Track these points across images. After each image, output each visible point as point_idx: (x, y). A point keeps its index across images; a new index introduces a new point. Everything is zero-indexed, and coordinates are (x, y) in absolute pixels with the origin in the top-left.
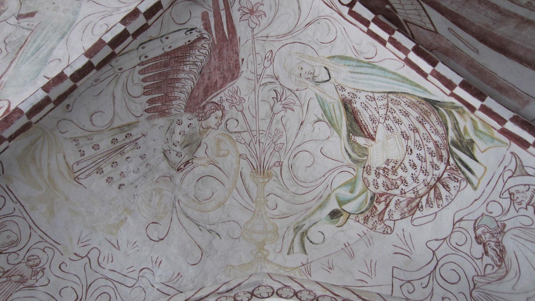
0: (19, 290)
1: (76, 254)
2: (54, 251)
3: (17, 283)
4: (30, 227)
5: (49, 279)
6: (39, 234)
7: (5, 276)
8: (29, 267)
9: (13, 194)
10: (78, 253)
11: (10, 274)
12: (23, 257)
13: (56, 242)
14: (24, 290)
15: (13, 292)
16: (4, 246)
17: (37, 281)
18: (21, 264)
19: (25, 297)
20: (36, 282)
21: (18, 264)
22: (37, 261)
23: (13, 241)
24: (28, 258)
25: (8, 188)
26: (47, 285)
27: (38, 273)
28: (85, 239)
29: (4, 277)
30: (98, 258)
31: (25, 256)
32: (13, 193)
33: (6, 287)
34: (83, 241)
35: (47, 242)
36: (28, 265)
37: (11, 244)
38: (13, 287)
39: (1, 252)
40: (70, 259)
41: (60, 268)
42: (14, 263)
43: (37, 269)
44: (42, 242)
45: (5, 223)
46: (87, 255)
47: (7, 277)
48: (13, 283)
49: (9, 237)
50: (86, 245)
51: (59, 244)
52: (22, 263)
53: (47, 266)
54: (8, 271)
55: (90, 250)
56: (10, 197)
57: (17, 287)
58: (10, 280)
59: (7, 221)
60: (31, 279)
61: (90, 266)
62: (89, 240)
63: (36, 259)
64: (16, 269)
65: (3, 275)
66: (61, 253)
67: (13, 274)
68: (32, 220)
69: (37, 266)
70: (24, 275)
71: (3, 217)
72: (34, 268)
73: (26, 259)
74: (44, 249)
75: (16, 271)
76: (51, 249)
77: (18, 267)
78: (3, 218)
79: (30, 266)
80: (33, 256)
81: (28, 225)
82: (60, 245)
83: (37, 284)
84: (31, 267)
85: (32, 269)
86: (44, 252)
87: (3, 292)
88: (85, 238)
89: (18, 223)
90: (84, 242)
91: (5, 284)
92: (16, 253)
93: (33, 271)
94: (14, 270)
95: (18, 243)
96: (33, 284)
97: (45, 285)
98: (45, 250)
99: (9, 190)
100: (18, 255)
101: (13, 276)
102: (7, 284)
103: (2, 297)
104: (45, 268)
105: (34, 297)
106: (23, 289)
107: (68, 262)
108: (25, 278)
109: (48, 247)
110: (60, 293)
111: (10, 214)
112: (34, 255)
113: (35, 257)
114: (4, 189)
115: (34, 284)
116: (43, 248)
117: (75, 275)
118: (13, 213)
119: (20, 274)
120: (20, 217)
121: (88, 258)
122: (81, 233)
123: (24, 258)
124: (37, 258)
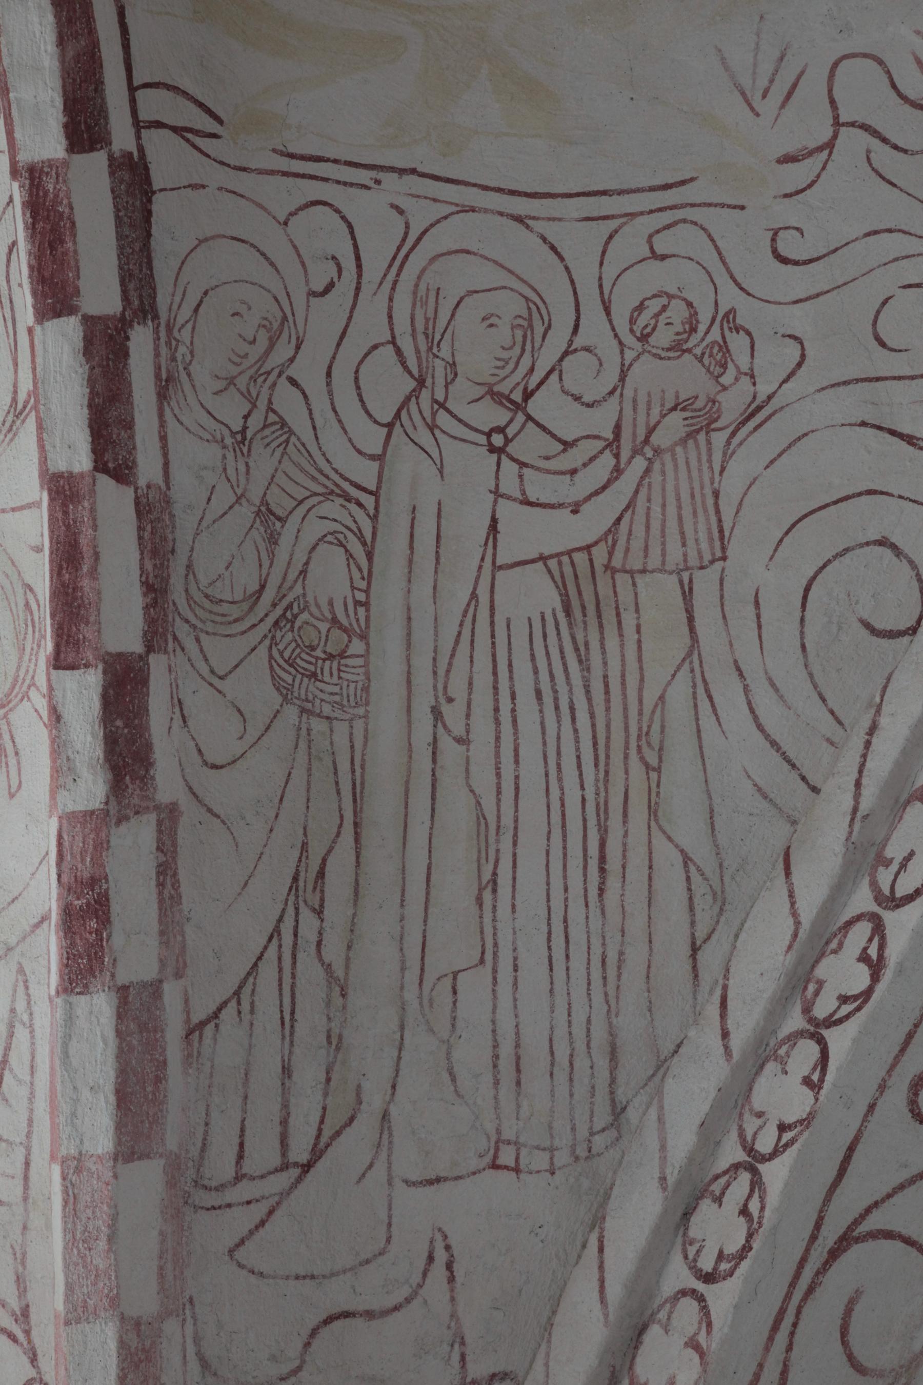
0: (725, 454)
1: (788, 159)
2: (695, 224)
3: (691, 443)
4: (519, 219)
5: (789, 332)
6: (576, 215)
7: (625, 454)
8: (671, 354)
9: (336, 161)
10: (790, 148)
11: (634, 434)
12: (615, 343)
13: (667, 187)
14: (741, 444)
15: (712, 483)
16: (511, 366)
17: (752, 376)
18: (636, 368)
19: (772, 462)
20: (754, 384)
21: (623, 378)
22: (678, 311)
23: (520, 321)
24: (632, 331)
25: (292, 156)
26: (803, 356)
27: (724, 347)
28: (766, 69)
29: (629, 462)
30: (894, 86)
31: (616, 336)
32: (328, 160)
33: (670, 487)
34: (763, 82)
35: (632, 215)
36: (660, 352)
37: (525, 337)
38: (694, 463)
39: (525, 389)
40: (786, 196)
41: (785, 261)
42: (610, 388)
43: (709, 339)
44: (616, 231)
45: (422, 287)
46: (836, 118)
47: (636, 452)
48: (679, 450)
49: (493, 320)
50: (795, 86)
51: (683, 183)
52: (636, 365)
53: (730, 297)
54: (617, 429)
55: (830, 91)
56: (338, 182)
57: (710, 455)
58: (657, 451)
59: (423, 271)
60: (725, 388)
61: (896, 147)
62: (782, 59)
63: (664, 308)
64: (635, 401)
65: (617, 456)
66: (729, 206)
67: (647, 423)
68: (499, 190)
69: (693, 330)
70: (683, 397)
71: (394, 270)
72: (690, 345)
73: (629, 340)
74: (652, 249)
75: (642, 407)
76: (681, 225)
77: (636, 391)
78: (398, 275)
79: (669, 350)
80: (641, 307)
81: (504, 220)
82: (692, 180)
83: (764, 389)
84: (678, 348)
85: (689, 351)
86: (663, 257)
87: (679, 507)
88: (755, 65)
89: (464, 246)
90: (772, 81)
91: (656, 477)
92: (576, 350)
93: (700, 359)
94: (635, 409)
95: (544, 312)
96: (750, 399)
97: (799, 365)
98: (660, 249)
99: (303, 158)
100: (587, 349)
101: (651, 431)
102: (663, 473)
103: (696, 523)
104: (732, 311)
105: (806, 435)
106: (736, 441)
107: (788, 212)
108: (699, 404)
109: (658, 232)
110: (883, 344)
111: (404, 240)
112: (642, 303)
113: (654, 306)
114: (285, 174)
115: (754, 398)
116: (647, 248)
117: (868, 234)
118: (407, 227)
119: (669, 405)
120: (446, 218)
121: (852, 124)
122: (723, 60)
123: (621, 343)
124: (664, 300)
